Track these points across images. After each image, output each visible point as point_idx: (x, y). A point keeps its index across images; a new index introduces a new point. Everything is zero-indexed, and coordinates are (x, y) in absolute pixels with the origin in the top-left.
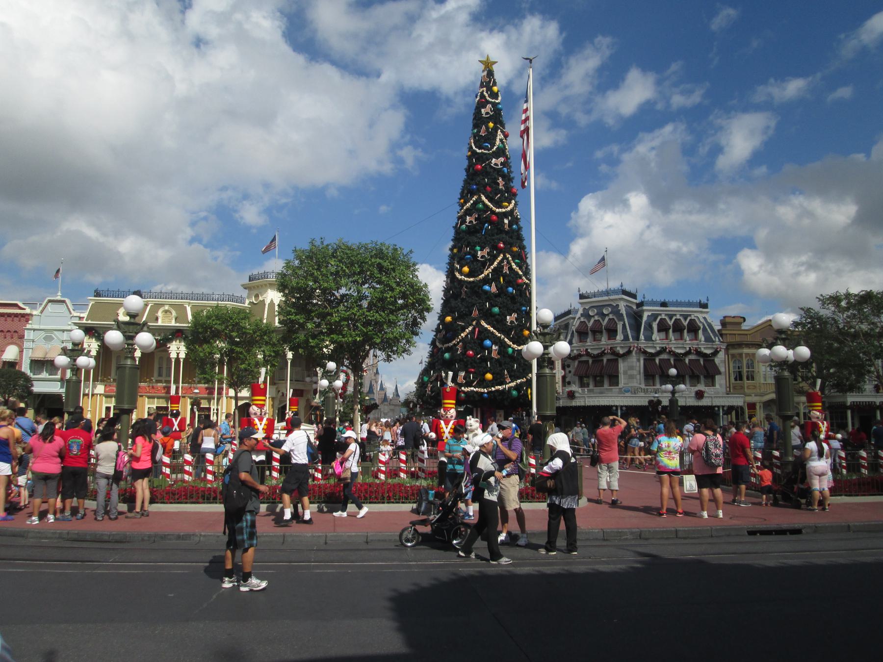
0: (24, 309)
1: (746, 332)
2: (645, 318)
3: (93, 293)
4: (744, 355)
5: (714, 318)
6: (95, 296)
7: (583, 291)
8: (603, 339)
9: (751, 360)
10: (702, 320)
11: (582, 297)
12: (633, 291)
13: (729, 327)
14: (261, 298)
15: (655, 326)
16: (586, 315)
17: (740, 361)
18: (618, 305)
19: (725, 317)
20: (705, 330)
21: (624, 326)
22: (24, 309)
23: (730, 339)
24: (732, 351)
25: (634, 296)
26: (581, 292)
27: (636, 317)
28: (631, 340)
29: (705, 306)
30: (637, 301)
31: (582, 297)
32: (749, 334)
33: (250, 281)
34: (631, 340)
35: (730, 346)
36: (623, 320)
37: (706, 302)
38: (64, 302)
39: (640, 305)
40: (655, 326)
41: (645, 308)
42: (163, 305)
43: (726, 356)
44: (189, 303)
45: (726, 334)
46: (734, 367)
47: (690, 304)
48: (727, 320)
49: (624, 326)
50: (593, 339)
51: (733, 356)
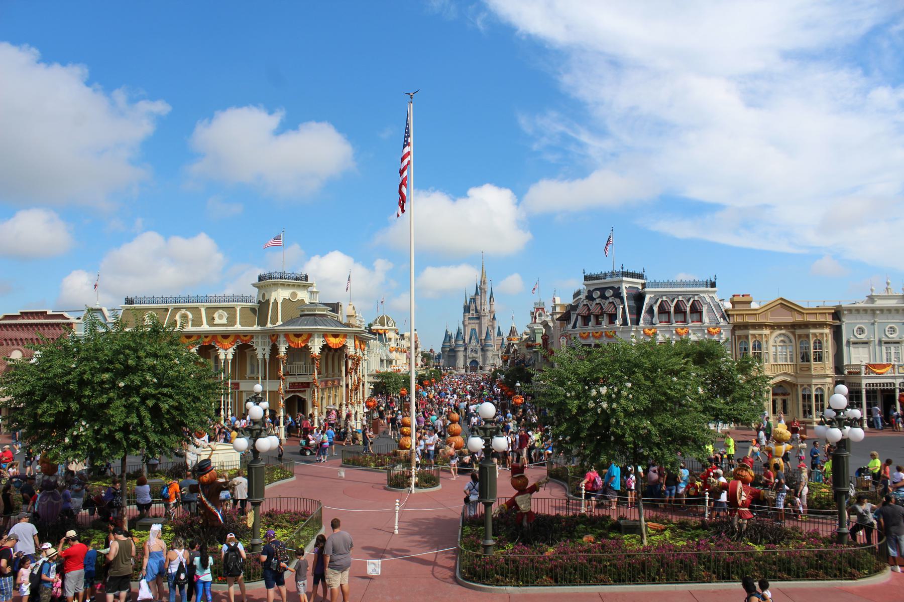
0: (69, 319)
1: (755, 312)
2: (647, 301)
3: (124, 301)
4: (750, 336)
5: (722, 297)
6: (126, 304)
7: (588, 273)
8: (603, 323)
9: (758, 341)
10: (708, 300)
11: (587, 278)
12: (639, 271)
13: (738, 307)
14: (267, 298)
15: (656, 309)
16: (590, 297)
17: (747, 343)
18: (619, 288)
19: (734, 296)
20: (710, 310)
21: (624, 309)
22: (69, 319)
23: (738, 320)
24: (738, 333)
25: (641, 276)
26: (585, 275)
27: (639, 298)
28: (630, 324)
29: (713, 285)
30: (642, 281)
31: (587, 278)
32: (759, 314)
33: (259, 281)
34: (630, 324)
35: (736, 327)
36: (623, 303)
37: (713, 280)
38: (101, 310)
39: (644, 285)
40: (656, 309)
41: (646, 290)
42: (179, 309)
43: (733, 337)
44: (203, 305)
45: (733, 315)
46: (741, 349)
47: (695, 284)
48: (736, 299)
49: (624, 309)
50: (595, 323)
51: (740, 337)
